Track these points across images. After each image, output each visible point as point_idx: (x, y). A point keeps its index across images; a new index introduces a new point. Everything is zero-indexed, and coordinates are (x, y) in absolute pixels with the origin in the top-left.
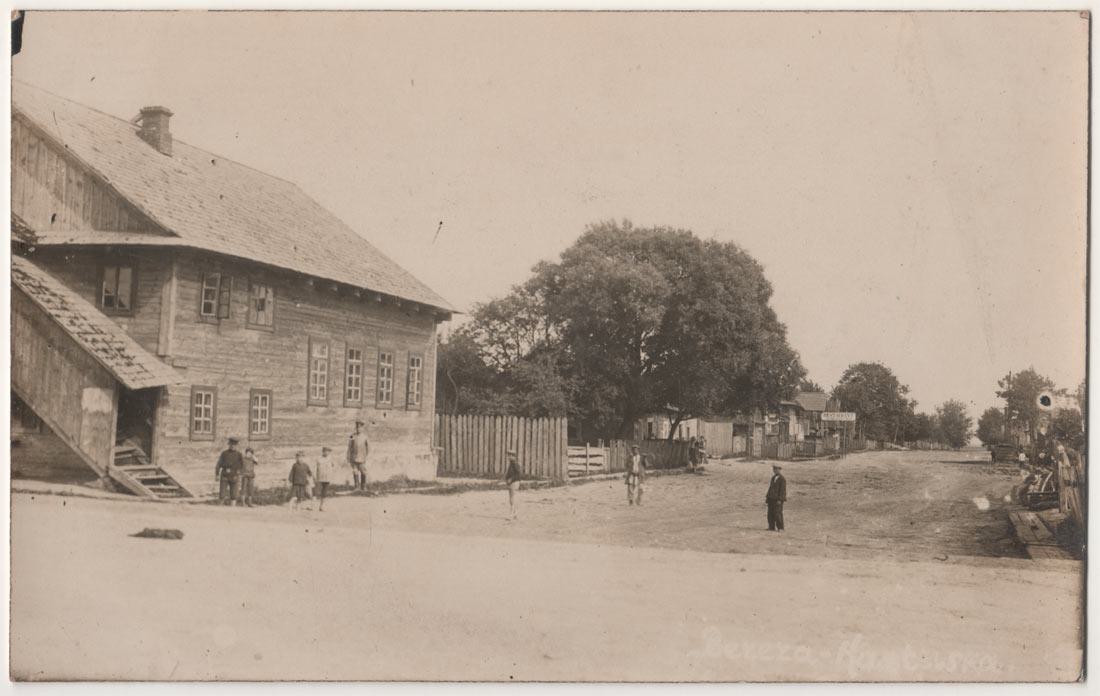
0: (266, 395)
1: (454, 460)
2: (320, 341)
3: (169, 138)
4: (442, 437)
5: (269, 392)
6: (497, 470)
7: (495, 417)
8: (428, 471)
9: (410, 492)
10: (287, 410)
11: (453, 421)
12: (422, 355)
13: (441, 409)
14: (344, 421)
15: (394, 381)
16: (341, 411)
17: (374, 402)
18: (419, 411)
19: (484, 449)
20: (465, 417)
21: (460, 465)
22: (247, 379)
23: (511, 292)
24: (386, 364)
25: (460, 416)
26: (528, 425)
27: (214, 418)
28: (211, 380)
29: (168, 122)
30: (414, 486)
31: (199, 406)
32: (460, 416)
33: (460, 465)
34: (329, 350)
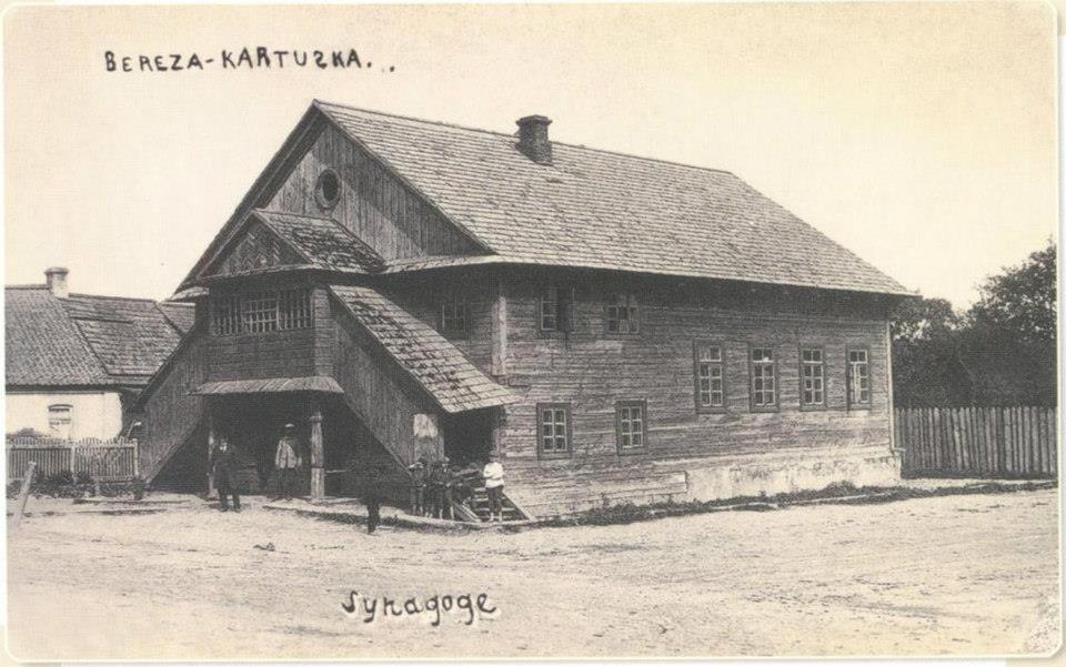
0: (637, 407)
1: (959, 458)
2: (704, 343)
3: (548, 146)
4: (904, 434)
5: (643, 404)
6: (1009, 467)
7: (1003, 408)
8: (888, 476)
9: (826, 503)
10: (661, 421)
11: (955, 416)
12: (868, 348)
13: (900, 401)
14: (753, 428)
15: (825, 380)
16: (747, 417)
17: (798, 404)
18: (870, 409)
19: (992, 445)
20: (968, 410)
21: (967, 464)
22: (612, 391)
23: (1029, 262)
24: (812, 362)
25: (962, 409)
26: (1043, 416)
27: (570, 435)
28: (563, 395)
29: (546, 130)
30: (875, 495)
31: (626, 420)
32: (962, 409)
33: (967, 464)
34: (723, 354)
